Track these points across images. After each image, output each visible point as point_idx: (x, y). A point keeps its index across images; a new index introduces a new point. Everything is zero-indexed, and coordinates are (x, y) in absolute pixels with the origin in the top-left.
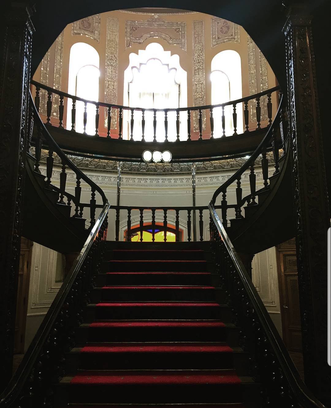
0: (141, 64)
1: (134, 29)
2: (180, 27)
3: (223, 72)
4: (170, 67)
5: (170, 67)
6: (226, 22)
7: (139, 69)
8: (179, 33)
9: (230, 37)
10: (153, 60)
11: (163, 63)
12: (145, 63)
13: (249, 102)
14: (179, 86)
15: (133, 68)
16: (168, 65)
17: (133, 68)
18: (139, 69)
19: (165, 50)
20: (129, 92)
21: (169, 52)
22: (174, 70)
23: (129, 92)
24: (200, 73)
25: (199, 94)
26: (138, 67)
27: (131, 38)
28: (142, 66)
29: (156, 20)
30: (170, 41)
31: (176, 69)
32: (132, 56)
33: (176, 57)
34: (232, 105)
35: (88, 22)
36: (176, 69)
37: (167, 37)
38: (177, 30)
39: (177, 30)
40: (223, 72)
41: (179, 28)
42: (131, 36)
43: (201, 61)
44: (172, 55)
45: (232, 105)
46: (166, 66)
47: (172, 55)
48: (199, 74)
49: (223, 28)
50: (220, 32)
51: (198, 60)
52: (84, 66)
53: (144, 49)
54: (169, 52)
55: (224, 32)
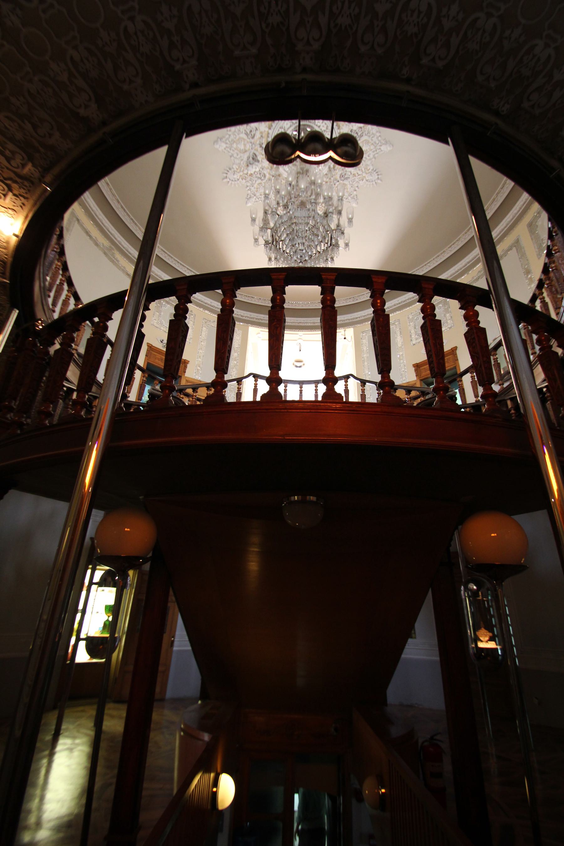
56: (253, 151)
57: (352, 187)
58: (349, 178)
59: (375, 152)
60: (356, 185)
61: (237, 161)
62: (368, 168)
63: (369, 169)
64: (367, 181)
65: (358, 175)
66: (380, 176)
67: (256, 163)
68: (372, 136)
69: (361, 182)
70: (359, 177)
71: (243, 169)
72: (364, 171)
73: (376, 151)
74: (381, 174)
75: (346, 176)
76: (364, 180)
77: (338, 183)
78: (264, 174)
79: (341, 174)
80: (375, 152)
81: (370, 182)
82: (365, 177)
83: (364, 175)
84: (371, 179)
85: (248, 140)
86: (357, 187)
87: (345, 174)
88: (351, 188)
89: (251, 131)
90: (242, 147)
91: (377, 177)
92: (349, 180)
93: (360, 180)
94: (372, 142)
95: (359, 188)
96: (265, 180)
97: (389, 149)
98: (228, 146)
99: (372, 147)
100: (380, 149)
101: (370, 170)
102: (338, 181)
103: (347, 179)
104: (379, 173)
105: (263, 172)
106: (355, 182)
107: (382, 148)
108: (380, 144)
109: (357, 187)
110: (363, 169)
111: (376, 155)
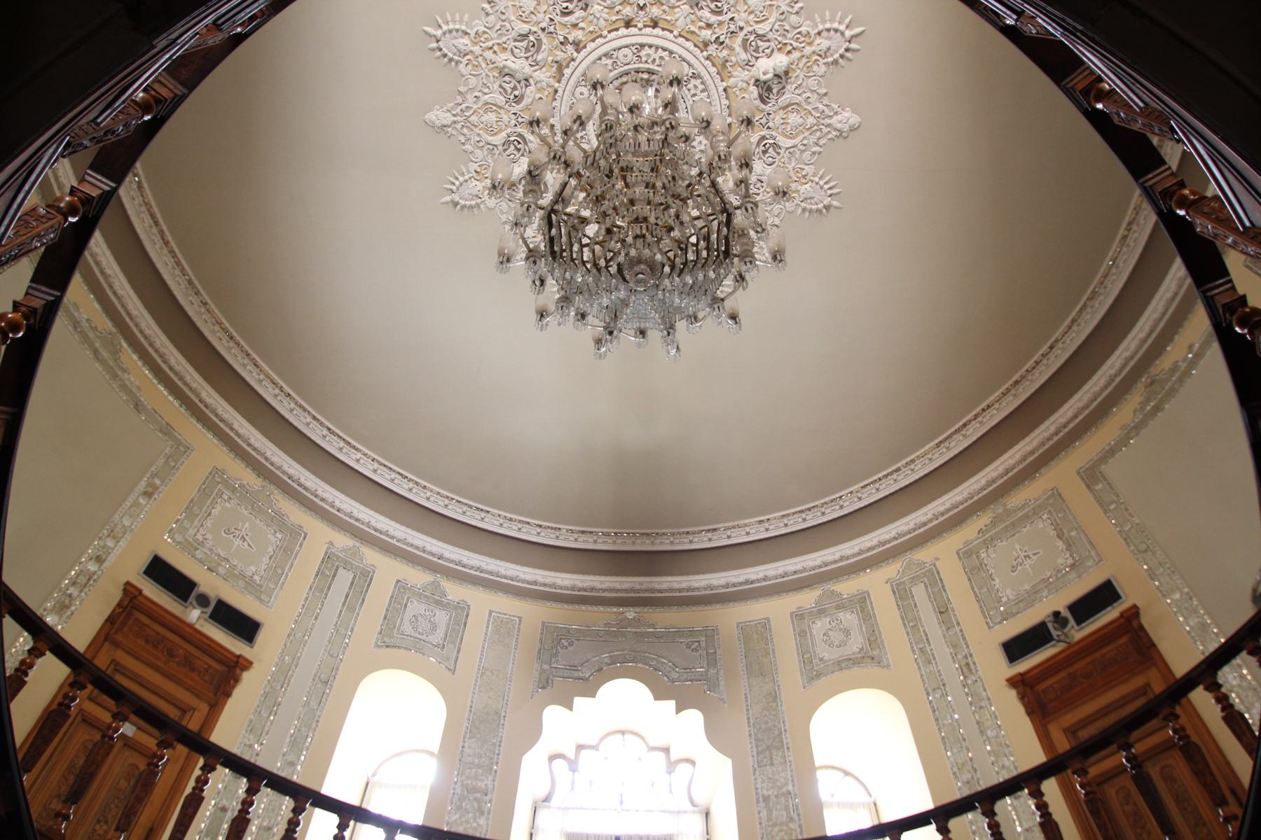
0: (580, 747)
1: (566, 644)
2: (703, 639)
3: (847, 773)
4: (674, 756)
5: (674, 756)
6: (837, 620)
7: (573, 765)
8: (698, 653)
9: (857, 656)
10: (619, 736)
11: (652, 744)
12: (594, 743)
13: (998, 806)
14: (707, 815)
15: (552, 758)
16: (667, 750)
17: (552, 758)
18: (573, 765)
19: (656, 699)
20: (531, 835)
21: (671, 704)
22: (688, 766)
23: (531, 835)
24: (775, 762)
25: (781, 831)
26: (571, 755)
27: (553, 666)
28: (584, 752)
29: (630, 623)
30: (674, 673)
31: (693, 763)
32: (553, 714)
33: (694, 717)
34: (933, 827)
35: (430, 621)
36: (693, 763)
37: (663, 663)
38: (693, 647)
39: (693, 647)
40: (847, 773)
41: (699, 642)
42: (553, 660)
43: (775, 726)
44: (678, 711)
45: (933, 827)
46: (662, 755)
47: (679, 710)
48: (772, 764)
49: (830, 633)
50: (824, 644)
51: (766, 723)
52: (398, 755)
53: (592, 693)
54: (671, 704)
55: (837, 643)
56: (767, 108)
57: (503, 14)
58: (515, 40)
59: (463, 106)
60: (492, 18)
61: (812, 83)
62: (470, 67)
63: (467, 64)
64: (466, 33)
65: (491, 48)
66: (434, 45)
67: (763, 78)
68: (481, 144)
69: (482, 29)
70: (490, 44)
71: (801, 65)
72: (480, 59)
73: (461, 110)
74: (433, 50)
75: (524, 44)
76: (472, 33)
77: (543, 25)
78: (746, 50)
79: (538, 51)
80: (463, 106)
81: (457, 31)
82: (475, 44)
83: (476, 49)
84: (456, 38)
85: (774, 133)
86: (487, 14)
87: (527, 50)
88: (502, 9)
89: (765, 152)
90: (794, 119)
91: (441, 44)
92: (514, 34)
93: (484, 32)
94: (477, 130)
95: (483, 9)
96: (745, 31)
97: (431, 116)
98: (827, 121)
99: (474, 118)
100: (454, 115)
101: (464, 61)
102: (543, 30)
103: (524, 36)
104: (439, 53)
105: (749, 55)
106: (498, 27)
107: (448, 119)
108: (459, 126)
109: (487, 14)
110: (484, 65)
111: (459, 100)
